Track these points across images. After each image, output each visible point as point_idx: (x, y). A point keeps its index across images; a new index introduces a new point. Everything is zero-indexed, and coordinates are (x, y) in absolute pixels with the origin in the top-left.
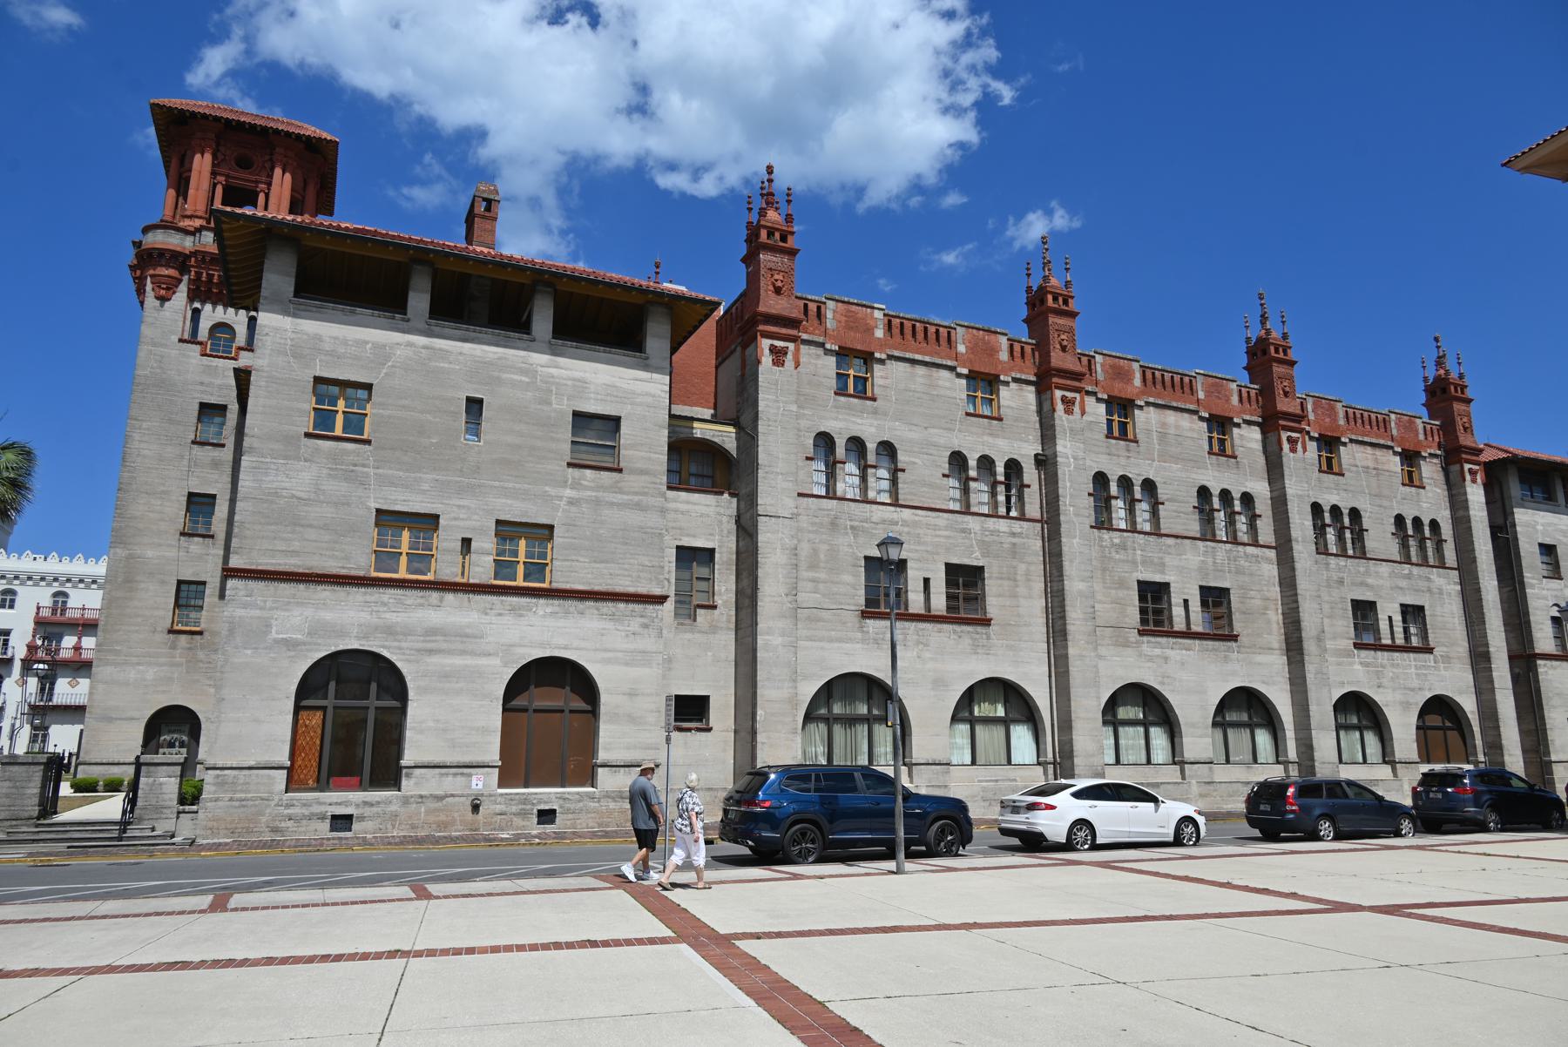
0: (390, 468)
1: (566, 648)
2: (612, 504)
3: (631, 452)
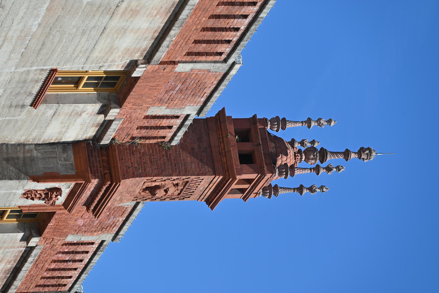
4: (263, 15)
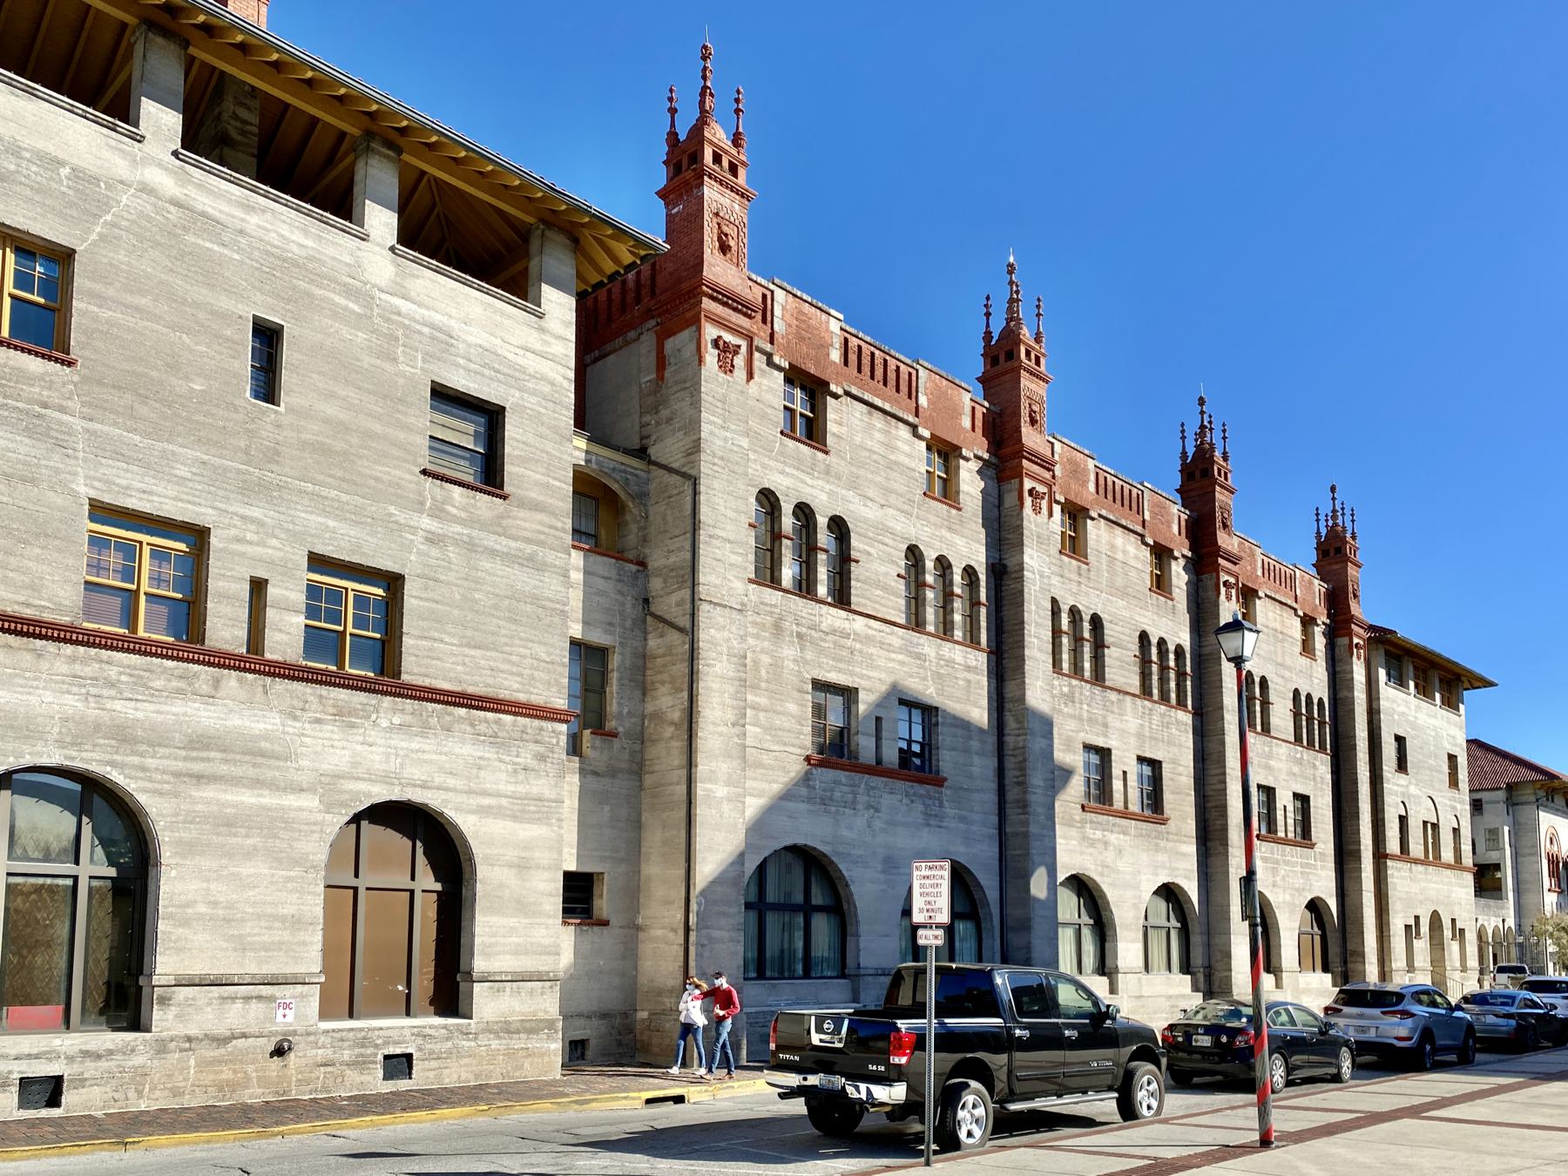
0: (115, 424)
1: (424, 786)
2: (493, 553)
3: (521, 470)
4: (1112, 472)
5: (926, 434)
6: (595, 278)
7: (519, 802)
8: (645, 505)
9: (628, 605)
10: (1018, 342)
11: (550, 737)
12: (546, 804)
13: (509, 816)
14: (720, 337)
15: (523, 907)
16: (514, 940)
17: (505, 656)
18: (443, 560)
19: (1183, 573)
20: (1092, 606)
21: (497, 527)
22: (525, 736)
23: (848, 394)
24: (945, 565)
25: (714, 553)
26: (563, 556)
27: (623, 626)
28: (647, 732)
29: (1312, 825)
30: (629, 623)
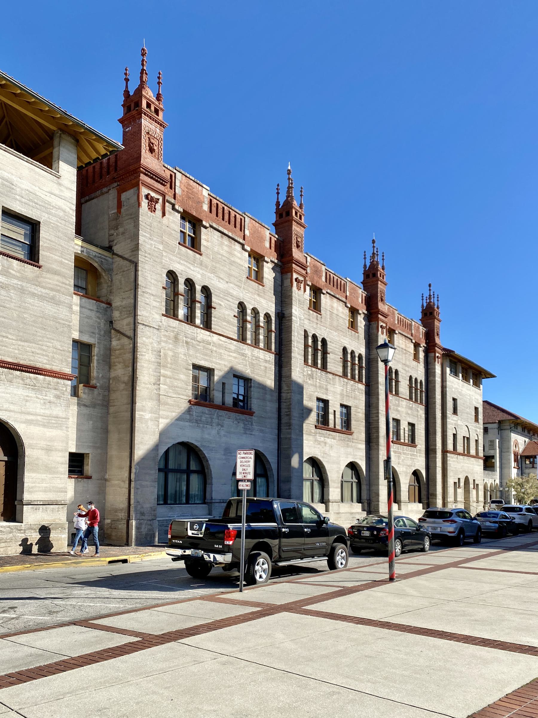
2: (33, 295)
4: (333, 272)
5: (248, 249)
6: (87, 160)
7: (47, 418)
8: (111, 275)
9: (102, 324)
10: (292, 207)
11: (62, 387)
12: (61, 420)
13: (42, 425)
14: (149, 194)
15: (48, 469)
16: (44, 485)
17: (39, 346)
18: (8, 297)
19: (363, 321)
20: (323, 334)
21: (36, 282)
22: (49, 386)
23: (211, 226)
24: (256, 312)
25: (145, 300)
26: (69, 298)
27: (99, 334)
28: (111, 386)
29: (416, 437)
30: (102, 332)
